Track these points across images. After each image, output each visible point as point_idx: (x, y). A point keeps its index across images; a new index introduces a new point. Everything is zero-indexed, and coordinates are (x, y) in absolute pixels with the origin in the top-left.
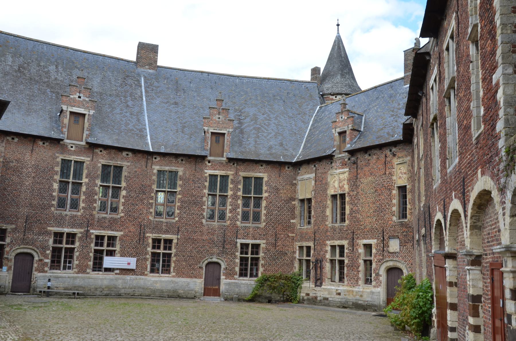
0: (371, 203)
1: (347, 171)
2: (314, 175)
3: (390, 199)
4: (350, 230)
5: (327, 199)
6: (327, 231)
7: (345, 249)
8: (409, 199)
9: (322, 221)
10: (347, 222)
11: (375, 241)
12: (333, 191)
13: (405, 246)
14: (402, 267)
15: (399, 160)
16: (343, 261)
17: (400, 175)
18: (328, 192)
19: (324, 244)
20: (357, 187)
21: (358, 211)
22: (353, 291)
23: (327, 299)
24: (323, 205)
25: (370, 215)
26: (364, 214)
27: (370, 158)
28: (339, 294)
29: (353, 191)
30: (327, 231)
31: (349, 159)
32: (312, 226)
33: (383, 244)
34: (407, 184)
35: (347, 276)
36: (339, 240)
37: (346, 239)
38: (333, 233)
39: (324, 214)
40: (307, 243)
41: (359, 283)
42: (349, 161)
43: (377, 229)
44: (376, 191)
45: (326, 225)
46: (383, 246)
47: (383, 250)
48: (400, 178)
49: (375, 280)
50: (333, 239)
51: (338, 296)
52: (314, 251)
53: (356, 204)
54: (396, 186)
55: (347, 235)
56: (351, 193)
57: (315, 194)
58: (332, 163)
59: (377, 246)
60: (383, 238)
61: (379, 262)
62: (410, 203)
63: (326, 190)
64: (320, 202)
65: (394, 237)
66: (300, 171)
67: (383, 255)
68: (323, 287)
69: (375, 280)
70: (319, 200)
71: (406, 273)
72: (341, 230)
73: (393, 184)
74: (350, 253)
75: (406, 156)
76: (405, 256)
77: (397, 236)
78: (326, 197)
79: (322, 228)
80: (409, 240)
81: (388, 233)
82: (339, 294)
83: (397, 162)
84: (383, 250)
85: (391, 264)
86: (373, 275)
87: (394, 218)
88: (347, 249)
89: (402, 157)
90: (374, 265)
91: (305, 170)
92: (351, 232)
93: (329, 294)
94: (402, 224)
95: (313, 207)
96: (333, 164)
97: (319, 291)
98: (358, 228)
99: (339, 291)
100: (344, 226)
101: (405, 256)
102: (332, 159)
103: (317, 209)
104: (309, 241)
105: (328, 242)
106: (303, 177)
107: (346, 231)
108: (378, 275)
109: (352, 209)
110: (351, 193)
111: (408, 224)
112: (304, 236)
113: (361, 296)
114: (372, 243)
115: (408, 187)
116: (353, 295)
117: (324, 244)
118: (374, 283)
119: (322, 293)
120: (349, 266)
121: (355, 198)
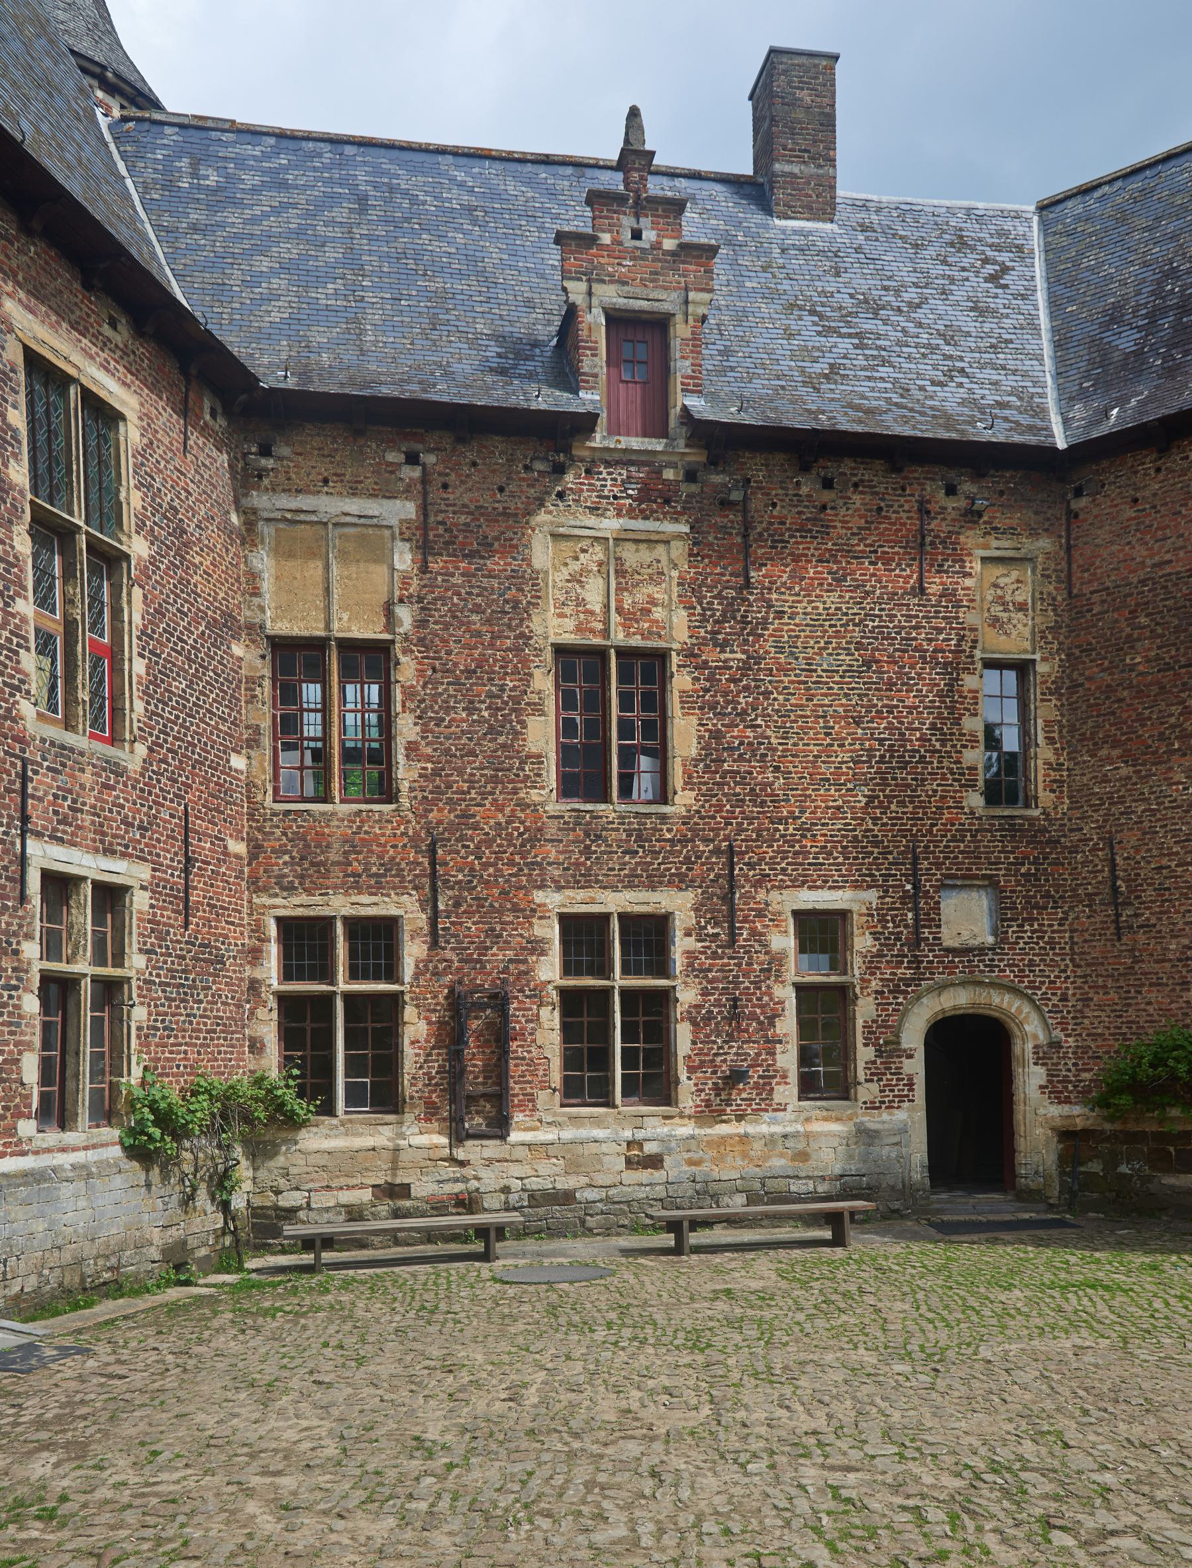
0: (836, 716)
1: (679, 536)
2: (408, 509)
3: (952, 710)
4: (706, 840)
5: (525, 662)
6: (535, 836)
7: (679, 934)
8: (1047, 723)
9: (494, 780)
10: (684, 800)
11: (872, 896)
12: (570, 624)
13: (1031, 920)
14: (1019, 1009)
15: (995, 543)
16: (664, 998)
17: (997, 610)
18: (536, 624)
19: (515, 909)
20: (751, 630)
21: (756, 751)
22: (744, 1138)
23: (567, 1197)
24: (491, 695)
25: (838, 772)
26: (795, 767)
27: (827, 496)
28: (654, 1162)
29: (723, 646)
30: (535, 836)
31: (691, 476)
32: (405, 801)
33: (916, 909)
34: (1037, 657)
35: (691, 1070)
36: (631, 886)
37: (681, 882)
38: (587, 851)
39: (504, 746)
40: (365, 899)
41: (777, 1098)
42: (694, 488)
43: (876, 844)
44: (867, 664)
45: (523, 805)
46: (916, 919)
47: (916, 941)
48: (995, 622)
49: (875, 1075)
50: (584, 879)
51: (644, 1175)
52: (434, 944)
53: (744, 712)
54: (978, 654)
55: (687, 860)
56: (711, 655)
57: (421, 624)
58: (559, 470)
59: (883, 921)
60: (916, 887)
61: (896, 991)
62: (1050, 740)
63: (519, 611)
64: (470, 673)
65: (964, 881)
66: (265, 462)
67: (916, 962)
68: (515, 1136)
69: (875, 1075)
70: (462, 660)
71: (1035, 1037)
72: (640, 838)
73: (966, 646)
74: (715, 955)
75: (1034, 534)
76: (1031, 963)
77: (989, 877)
78: (517, 650)
79: (488, 818)
80: (1047, 895)
81: (938, 866)
82: (654, 1162)
83: (986, 547)
84: (916, 941)
85: (958, 999)
86: (864, 1054)
87: (975, 800)
88: (696, 932)
89: (1011, 531)
90: (865, 1010)
91: (324, 469)
92: (717, 852)
93: (573, 1167)
94: (1011, 828)
95: (409, 693)
96: (569, 477)
97: (489, 1162)
98: (759, 832)
99: (650, 1148)
100: (664, 817)
101: (1031, 963)
102: (567, 450)
103: (448, 710)
104: (379, 886)
105: (553, 900)
106: (304, 502)
107: (684, 841)
108: (890, 1050)
109: (717, 735)
110: (711, 655)
111: (1044, 830)
112: (333, 856)
113: (803, 1156)
114: (855, 908)
115: (1042, 668)
116: (745, 1155)
117: (515, 909)
118: (867, 1091)
119: (516, 1170)
120: (709, 1017)
121: (732, 680)
